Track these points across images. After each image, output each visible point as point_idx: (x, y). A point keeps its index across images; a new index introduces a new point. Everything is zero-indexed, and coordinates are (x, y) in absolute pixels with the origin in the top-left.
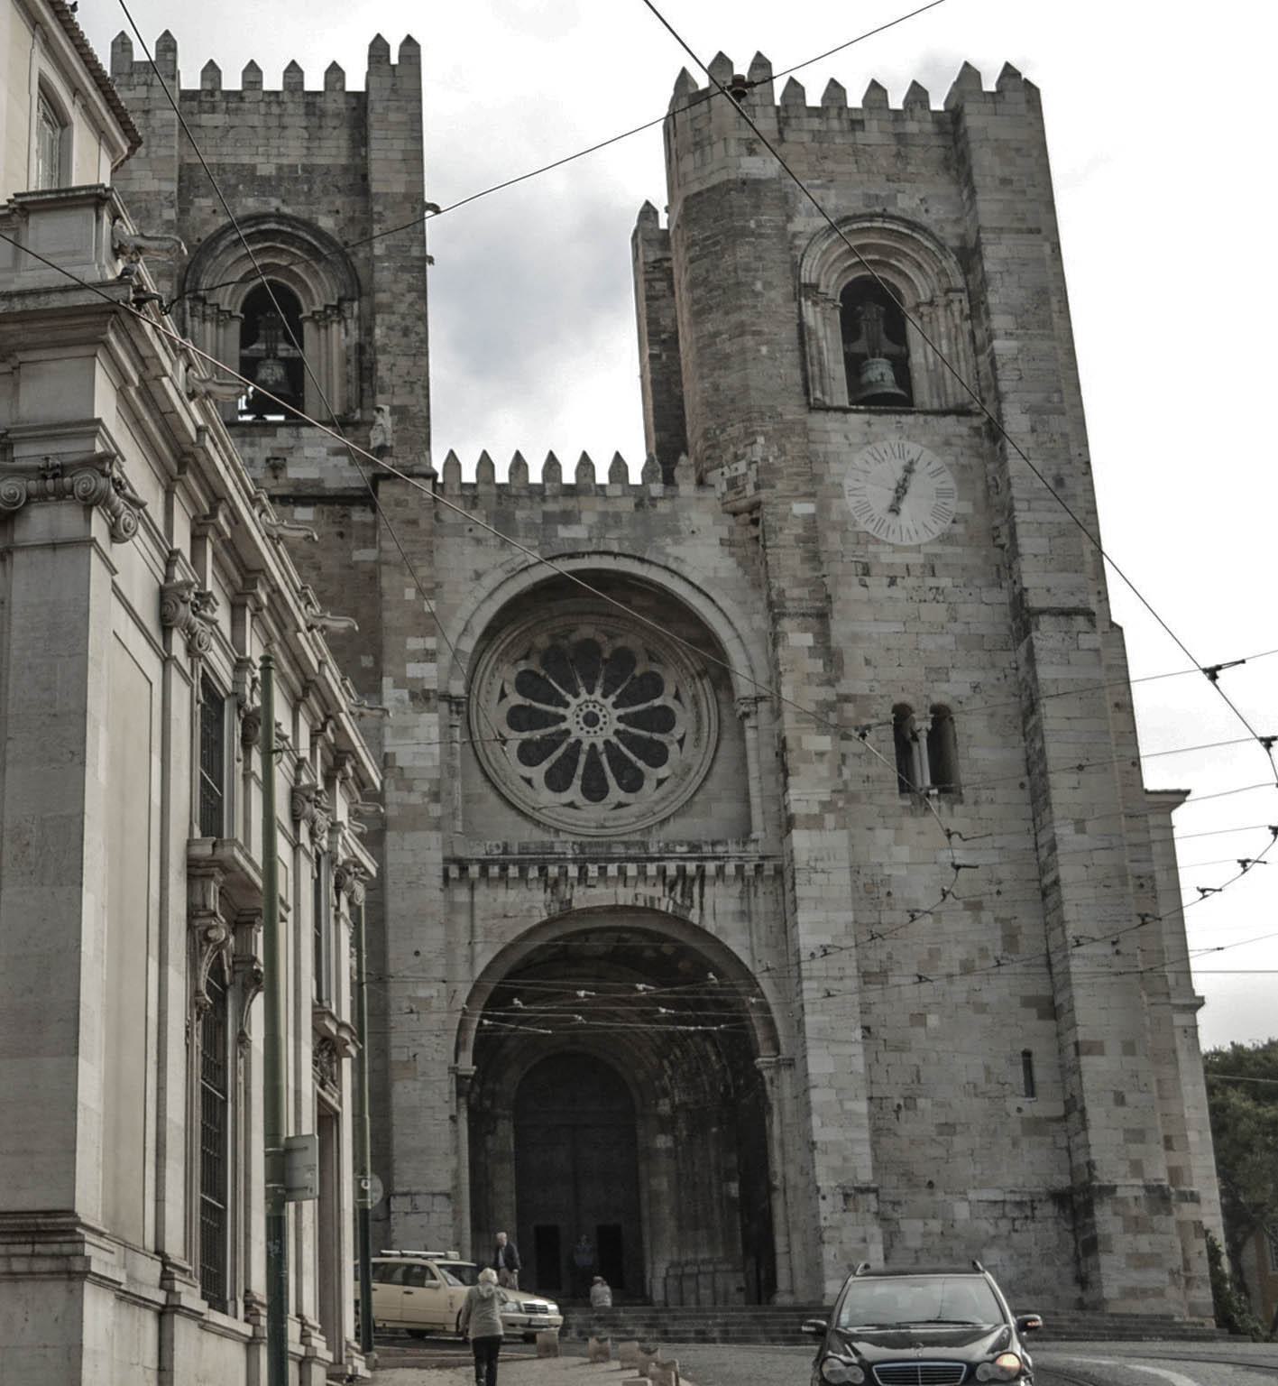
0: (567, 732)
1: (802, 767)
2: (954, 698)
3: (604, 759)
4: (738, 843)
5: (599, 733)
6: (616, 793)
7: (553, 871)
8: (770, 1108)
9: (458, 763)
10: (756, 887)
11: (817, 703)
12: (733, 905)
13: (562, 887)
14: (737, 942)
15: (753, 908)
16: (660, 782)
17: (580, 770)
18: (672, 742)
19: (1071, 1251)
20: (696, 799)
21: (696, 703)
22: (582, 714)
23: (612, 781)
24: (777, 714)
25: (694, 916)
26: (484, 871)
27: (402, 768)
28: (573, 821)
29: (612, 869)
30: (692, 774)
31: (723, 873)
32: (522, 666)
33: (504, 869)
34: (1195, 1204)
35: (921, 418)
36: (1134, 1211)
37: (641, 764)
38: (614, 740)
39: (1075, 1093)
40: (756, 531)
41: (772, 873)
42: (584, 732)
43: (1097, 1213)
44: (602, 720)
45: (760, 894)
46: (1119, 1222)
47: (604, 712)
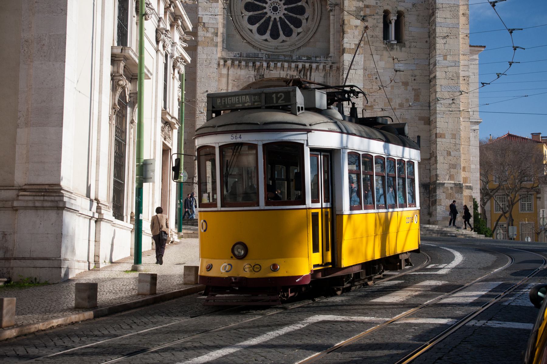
0: (266, 13)
2: (406, 8)
3: (279, 24)
4: (324, 57)
5: (278, 14)
6: (282, 37)
7: (258, 64)
10: (330, 74)
13: (261, 70)
15: (328, 81)
16: (298, 34)
17: (270, 28)
18: (304, 19)
19: (428, 204)
20: (311, 41)
22: (272, 7)
23: (281, 32)
24: (342, 10)
27: (204, 23)
28: (267, 46)
29: (279, 64)
30: (310, 31)
31: (318, 68)
33: (240, 62)
34: (471, 190)
36: (450, 191)
37: (292, 26)
38: (283, 17)
39: (434, 151)
41: (336, 68)
42: (272, 13)
43: (438, 192)
44: (279, 9)
45: (331, 76)
46: (444, 195)
47: (280, 6)
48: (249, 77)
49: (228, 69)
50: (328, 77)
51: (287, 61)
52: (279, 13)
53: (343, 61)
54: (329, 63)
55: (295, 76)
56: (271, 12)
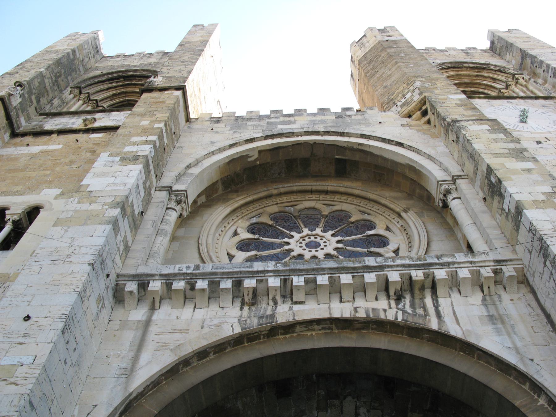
0: (291, 250)
1: (513, 177)
7: (250, 283)
9: (169, 228)
10: (500, 296)
11: (509, 149)
13: (264, 305)
15: (502, 312)
18: (387, 252)
21: (405, 229)
22: (304, 243)
26: (169, 286)
27: (91, 192)
32: (255, 220)
35: (522, 101)
41: (514, 273)
47: (325, 240)
48: (219, 325)
49: (153, 308)
50: (498, 303)
52: (322, 249)
53: (531, 225)
54: (487, 264)
55: (385, 311)
56: (304, 249)
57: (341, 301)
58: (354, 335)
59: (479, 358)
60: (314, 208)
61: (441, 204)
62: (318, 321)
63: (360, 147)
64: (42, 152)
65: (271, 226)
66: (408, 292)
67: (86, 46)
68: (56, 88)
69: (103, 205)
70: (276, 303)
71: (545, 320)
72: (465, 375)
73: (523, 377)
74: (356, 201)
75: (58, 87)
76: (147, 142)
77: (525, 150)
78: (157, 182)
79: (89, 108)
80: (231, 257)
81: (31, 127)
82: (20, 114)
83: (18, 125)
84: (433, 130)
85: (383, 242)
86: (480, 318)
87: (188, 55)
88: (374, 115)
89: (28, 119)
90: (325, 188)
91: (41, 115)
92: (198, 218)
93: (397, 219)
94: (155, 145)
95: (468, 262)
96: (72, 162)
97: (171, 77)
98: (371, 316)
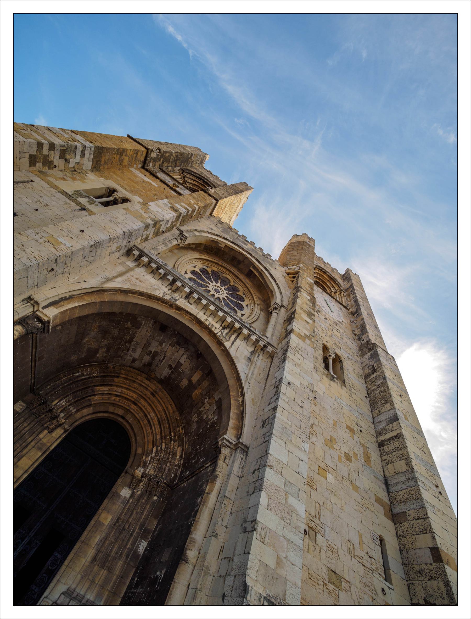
0: (208, 287)
1: (300, 320)
7: (179, 284)
8: (216, 477)
12: (248, 354)
14: (241, 366)
15: (255, 360)
18: (239, 313)
21: (252, 310)
22: (215, 288)
25: (227, 344)
26: (150, 262)
32: (206, 268)
38: (222, 299)
40: (292, 279)
41: (270, 352)
44: (221, 293)
47: (223, 292)
51: (216, 305)
53: (289, 340)
54: (264, 341)
55: (216, 328)
57: (204, 314)
58: (199, 328)
59: (233, 369)
60: (229, 279)
61: (270, 311)
62: (191, 314)
63: (261, 271)
64: (148, 182)
65: (209, 274)
66: (230, 329)
67: (198, 157)
68: (174, 163)
69: (149, 217)
70: (182, 297)
71: (267, 375)
72: (223, 370)
73: (241, 386)
74: (245, 289)
75: (175, 164)
76: (186, 208)
77: (314, 316)
78: (179, 226)
79: (181, 182)
80: (186, 273)
81: (152, 170)
82: (152, 161)
83: (148, 165)
84: (291, 285)
85: (241, 308)
86: (245, 356)
87: (231, 191)
88: (277, 265)
89: (154, 166)
90: (238, 276)
91: (160, 168)
92: (186, 251)
93: (253, 305)
94: (188, 212)
95: (258, 335)
96: (156, 195)
97: (217, 193)
98: (210, 326)
